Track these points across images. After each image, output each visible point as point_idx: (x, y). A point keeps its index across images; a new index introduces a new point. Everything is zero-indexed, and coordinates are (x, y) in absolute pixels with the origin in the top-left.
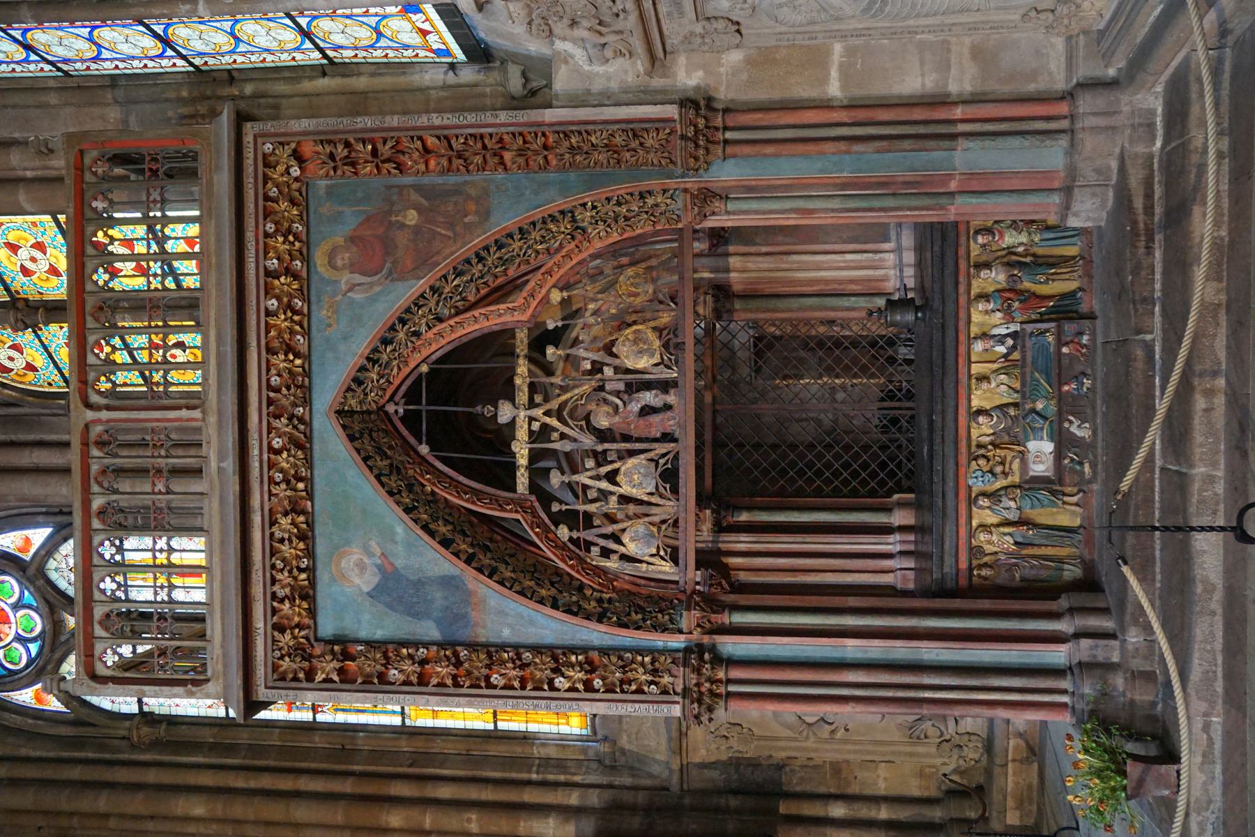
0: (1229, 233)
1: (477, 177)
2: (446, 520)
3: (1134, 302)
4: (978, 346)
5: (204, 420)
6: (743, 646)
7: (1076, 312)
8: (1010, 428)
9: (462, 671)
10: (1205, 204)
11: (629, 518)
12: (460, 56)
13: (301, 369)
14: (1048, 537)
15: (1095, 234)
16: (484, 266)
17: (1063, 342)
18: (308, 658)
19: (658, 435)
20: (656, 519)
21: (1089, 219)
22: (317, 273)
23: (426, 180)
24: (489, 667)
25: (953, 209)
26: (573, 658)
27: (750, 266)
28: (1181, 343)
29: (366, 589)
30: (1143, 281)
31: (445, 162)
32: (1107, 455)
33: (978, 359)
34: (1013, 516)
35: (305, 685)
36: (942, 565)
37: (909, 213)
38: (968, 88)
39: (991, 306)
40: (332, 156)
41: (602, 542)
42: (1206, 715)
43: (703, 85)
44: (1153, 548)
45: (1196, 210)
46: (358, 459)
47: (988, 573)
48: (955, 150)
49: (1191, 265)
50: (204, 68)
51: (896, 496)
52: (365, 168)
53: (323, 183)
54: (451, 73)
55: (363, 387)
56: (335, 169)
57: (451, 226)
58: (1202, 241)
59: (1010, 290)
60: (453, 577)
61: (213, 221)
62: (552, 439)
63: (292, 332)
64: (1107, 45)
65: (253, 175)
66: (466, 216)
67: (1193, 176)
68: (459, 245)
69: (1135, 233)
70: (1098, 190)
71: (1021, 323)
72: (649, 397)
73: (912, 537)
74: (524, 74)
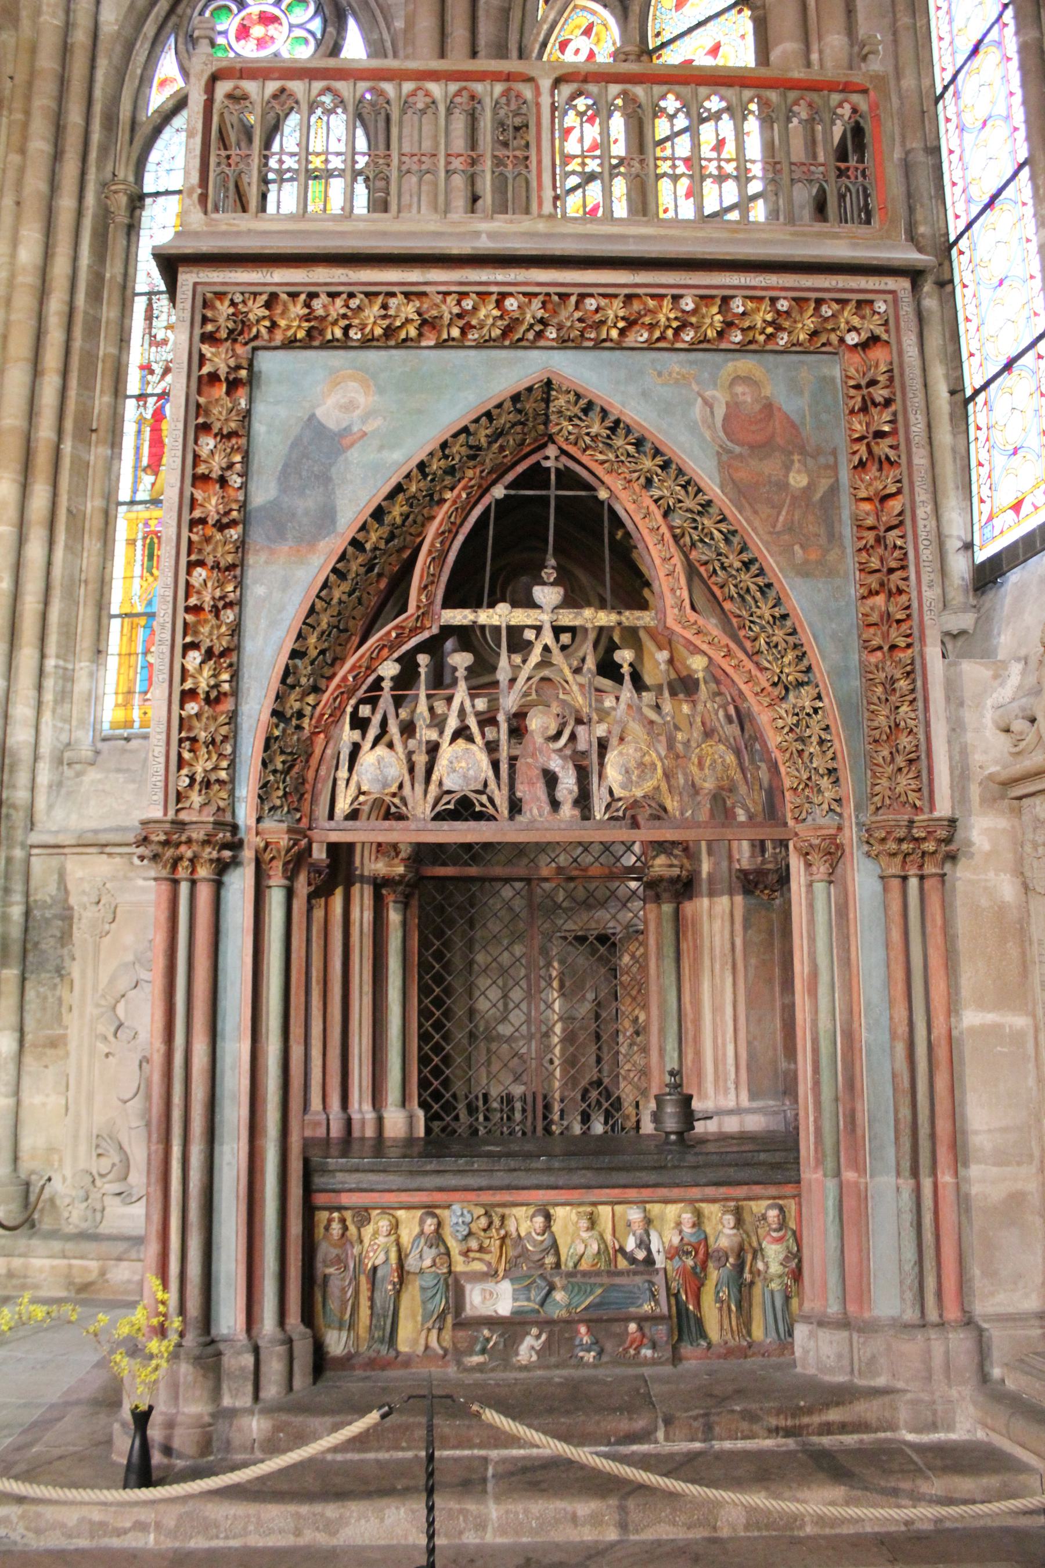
0: (808, 1537)
1: (850, 563)
2: (407, 517)
3: (706, 1415)
4: (634, 1214)
5: (540, 216)
6: (240, 903)
7: (680, 1339)
9: (210, 531)
10: (847, 1504)
11: (410, 754)
12: (981, 556)
13: (604, 336)
16: (738, 570)
18: (233, 336)
19: (519, 794)
20: (407, 791)
21: (806, 1352)
22: (727, 361)
23: (845, 499)
24: (216, 566)
25: (819, 1175)
26: (225, 676)
27: (717, 925)
29: (319, 413)
30: (733, 1427)
31: (870, 521)
34: (412, 1263)
35: (198, 332)
37: (811, 1119)
38: (975, 1190)
39: (687, 1229)
40: (873, 383)
41: (376, 720)
42: (158, 1526)
43: (973, 849)
44: (379, 1449)
45: (839, 1492)
46: (489, 406)
49: (767, 1489)
50: (954, 252)
51: (420, 1114)
52: (860, 423)
53: (837, 372)
54: (960, 544)
55: (581, 415)
56: (858, 387)
57: (790, 529)
58: (798, 1501)
59: (707, 1255)
60: (333, 521)
61: (788, 237)
62: (513, 656)
63: (652, 327)
65: (848, 287)
66: (802, 546)
67: (883, 1483)
68: (766, 537)
69: (797, 1412)
70: (846, 1362)
71: (665, 1269)
72: (568, 784)
73: (370, 1132)
74: (963, 633)
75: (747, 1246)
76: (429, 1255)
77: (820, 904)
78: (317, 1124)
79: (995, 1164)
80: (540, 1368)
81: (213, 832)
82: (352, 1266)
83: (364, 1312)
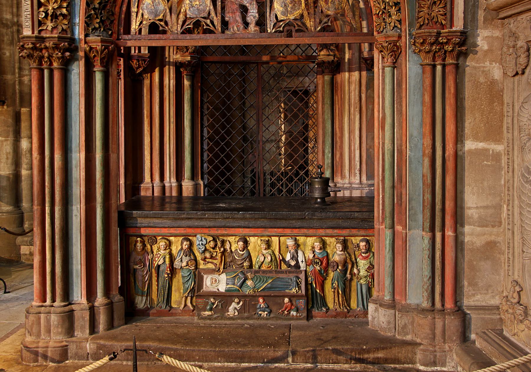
6: (78, 80)
7: (313, 307)
15: (365, 319)
25: (383, 227)
33: (281, 242)
34: (177, 264)
36: (142, 217)
37: (381, 196)
38: (467, 239)
39: (317, 251)
47: (138, 247)
48: (423, 230)
64: (490, 335)
71: (306, 271)
75: (348, 260)
76: (186, 260)
77: (388, 80)
79: (479, 226)
81: (58, 43)
82: (148, 264)
83: (154, 287)
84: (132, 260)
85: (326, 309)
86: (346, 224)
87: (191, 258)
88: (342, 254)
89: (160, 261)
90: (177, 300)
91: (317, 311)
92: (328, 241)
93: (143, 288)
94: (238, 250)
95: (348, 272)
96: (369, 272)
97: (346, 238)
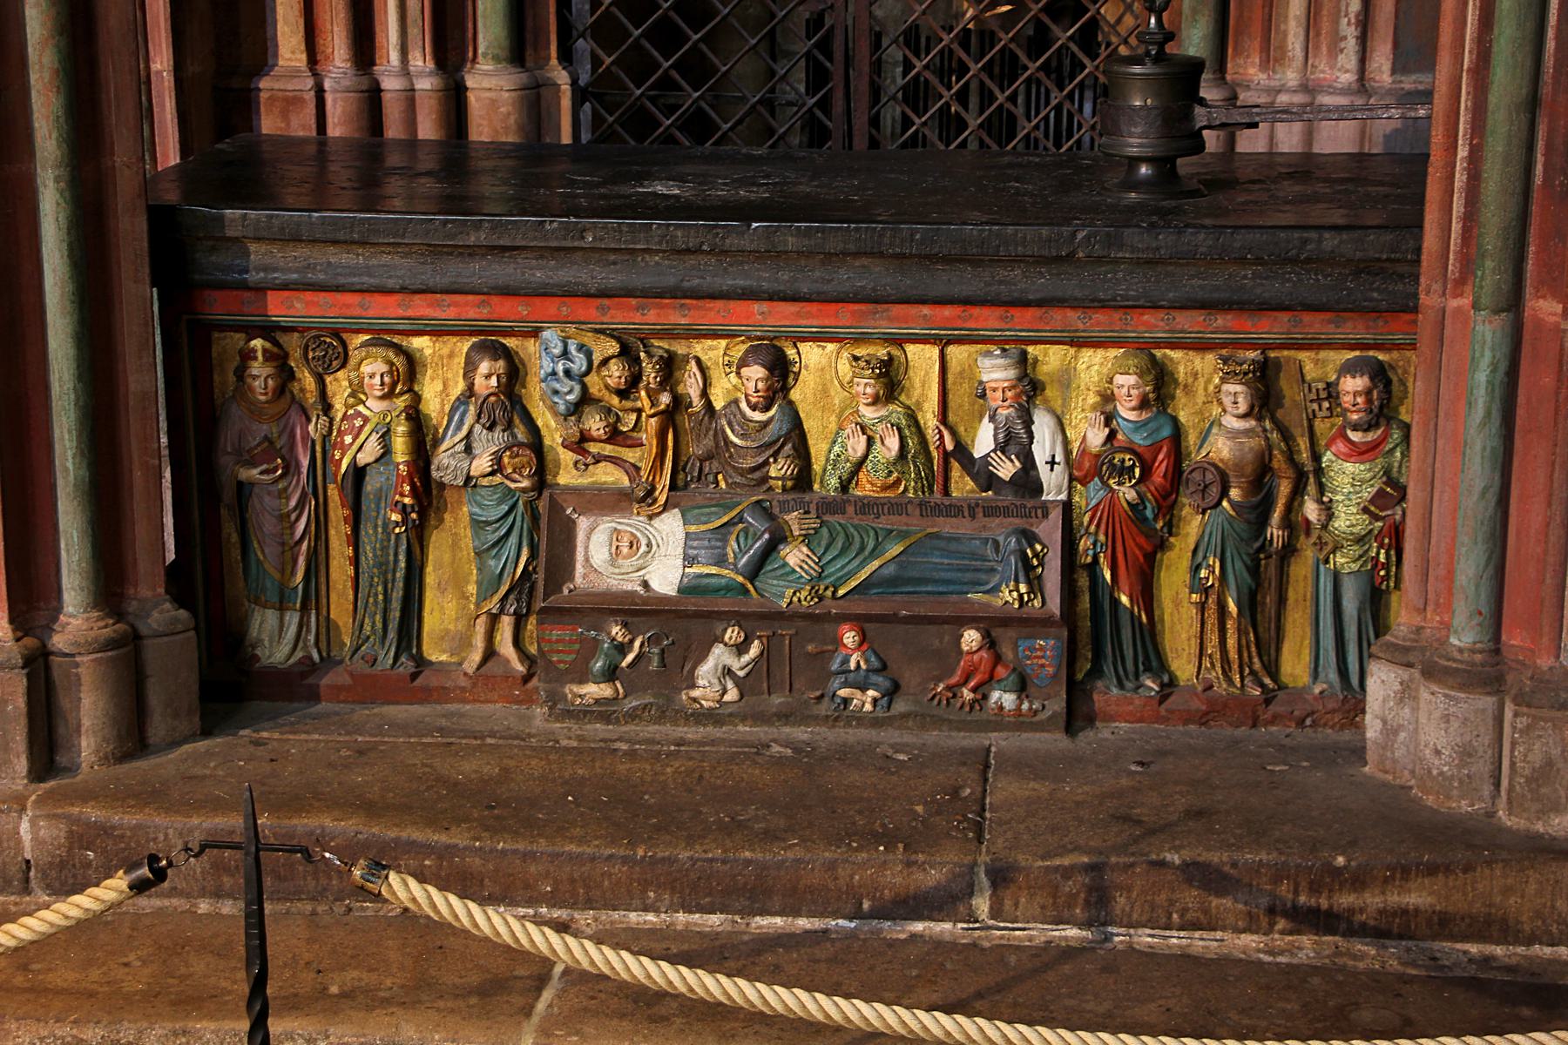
7: (1096, 672)
8: (728, 466)
14: (385, 569)
17: (996, 632)
21: (1390, 731)
25: (1465, 302)
28: (949, 1010)
30: (1163, 897)
32: (632, 755)
34: (447, 462)
37: (1462, 152)
39: (1126, 412)
51: (562, 77)
70: (1482, 767)
71: (1067, 506)
73: (428, 128)
75: (1278, 461)
78: (291, 103)
80: (744, 719)
82: (305, 462)
84: (228, 440)
85: (1162, 686)
86: (1274, 288)
87: (514, 436)
88: (1247, 433)
89: (368, 447)
90: (447, 631)
91: (1115, 691)
92: (1181, 369)
93: (283, 572)
94: (744, 405)
95: (1276, 516)
96: (1376, 518)
97: (1272, 354)
